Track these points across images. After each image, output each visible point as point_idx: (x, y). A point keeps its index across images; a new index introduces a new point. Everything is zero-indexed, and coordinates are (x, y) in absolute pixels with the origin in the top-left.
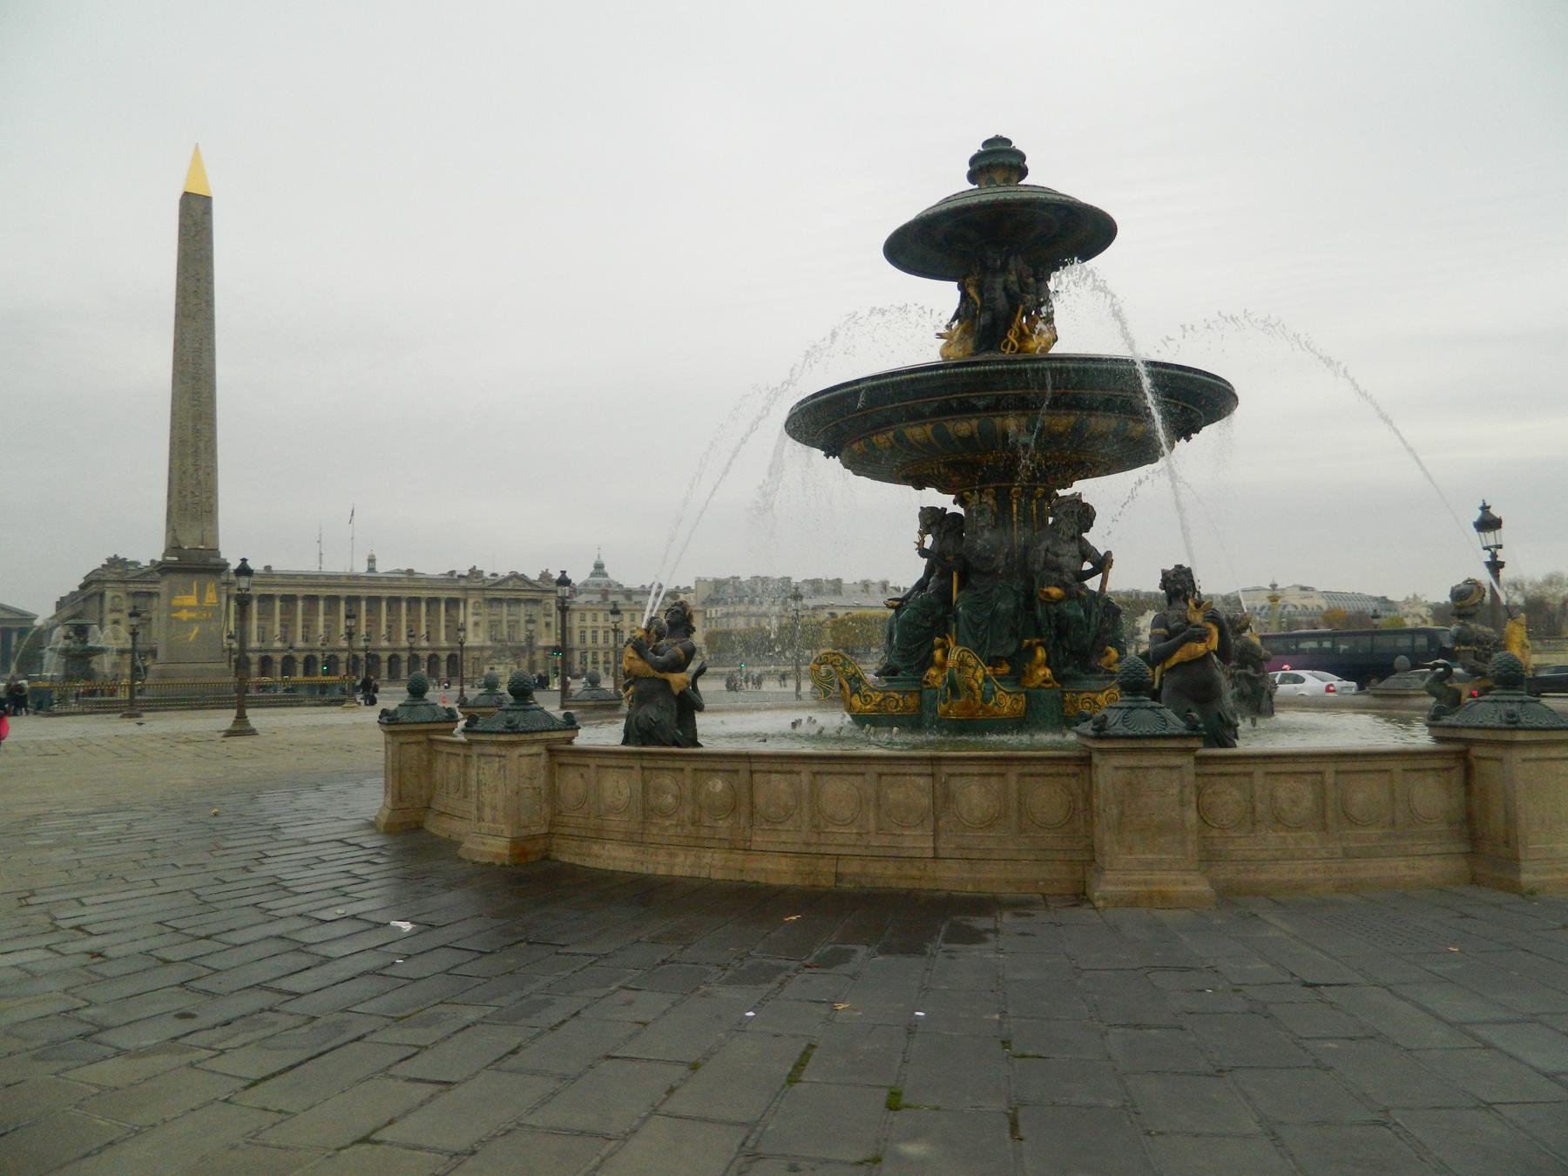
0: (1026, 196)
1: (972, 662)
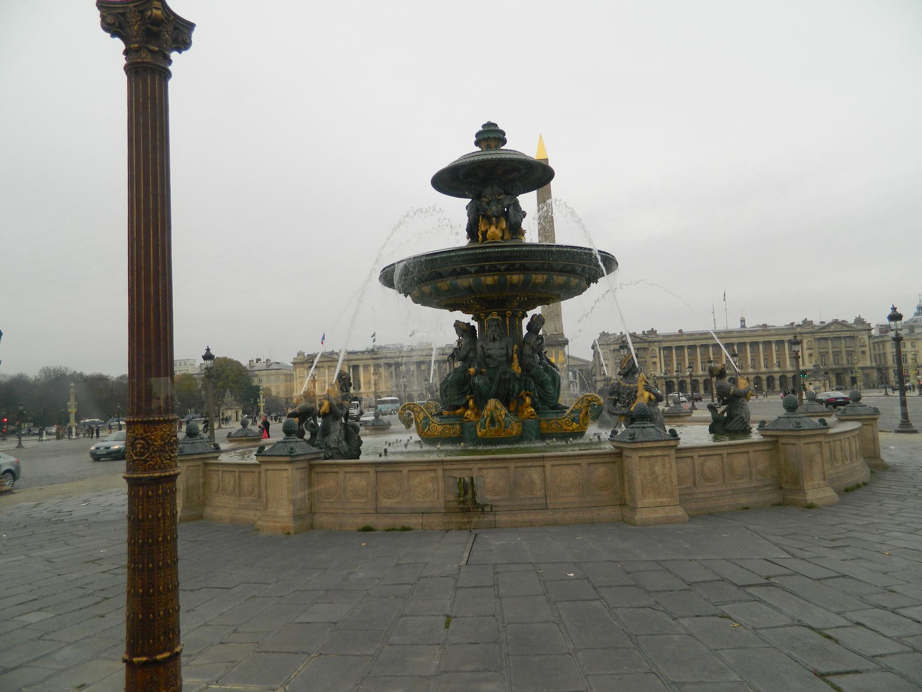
0: (503, 156)
1: (499, 406)
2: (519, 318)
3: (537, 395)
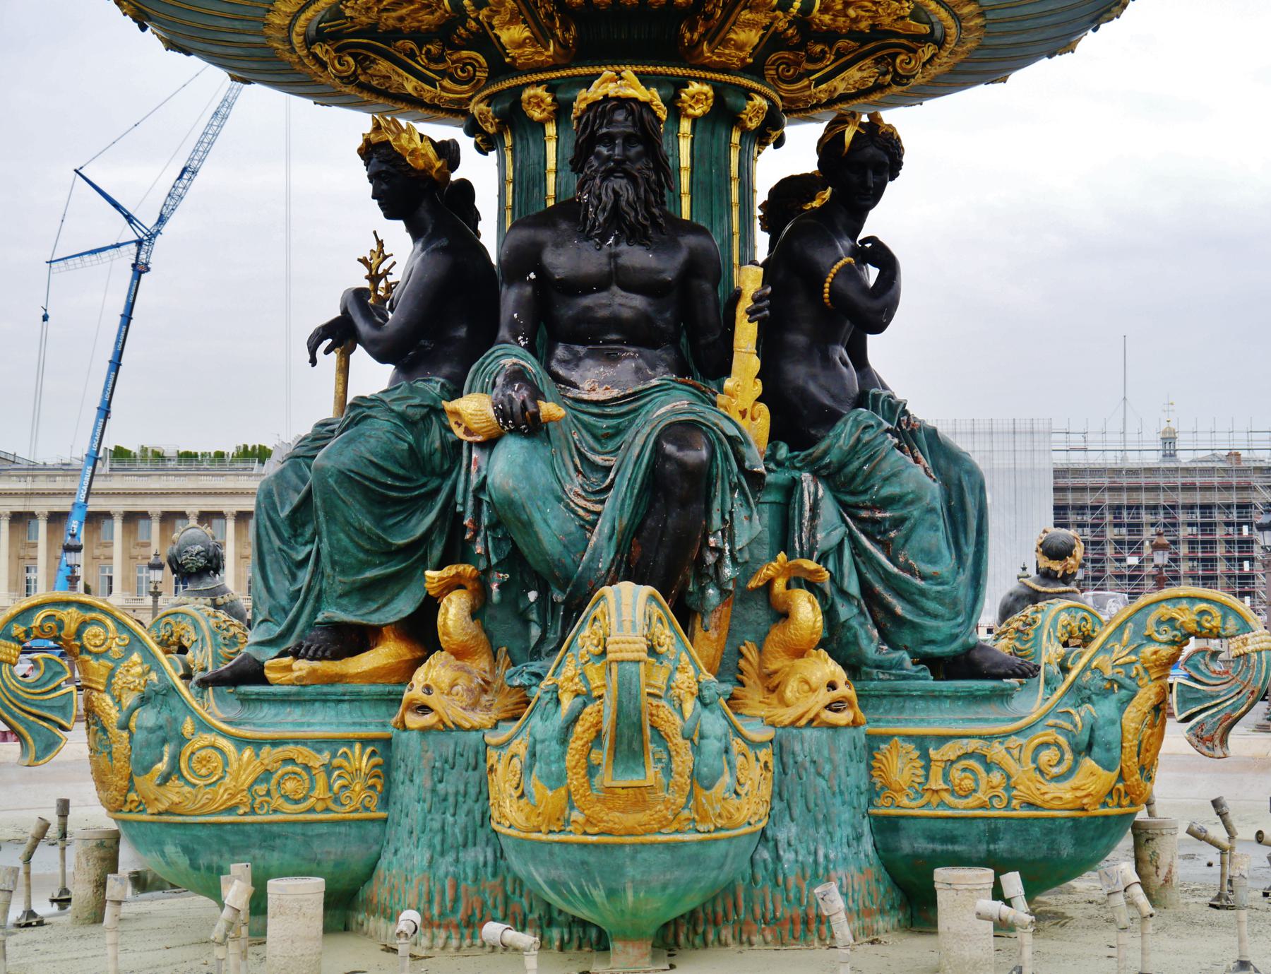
2: (745, 132)
3: (853, 586)
